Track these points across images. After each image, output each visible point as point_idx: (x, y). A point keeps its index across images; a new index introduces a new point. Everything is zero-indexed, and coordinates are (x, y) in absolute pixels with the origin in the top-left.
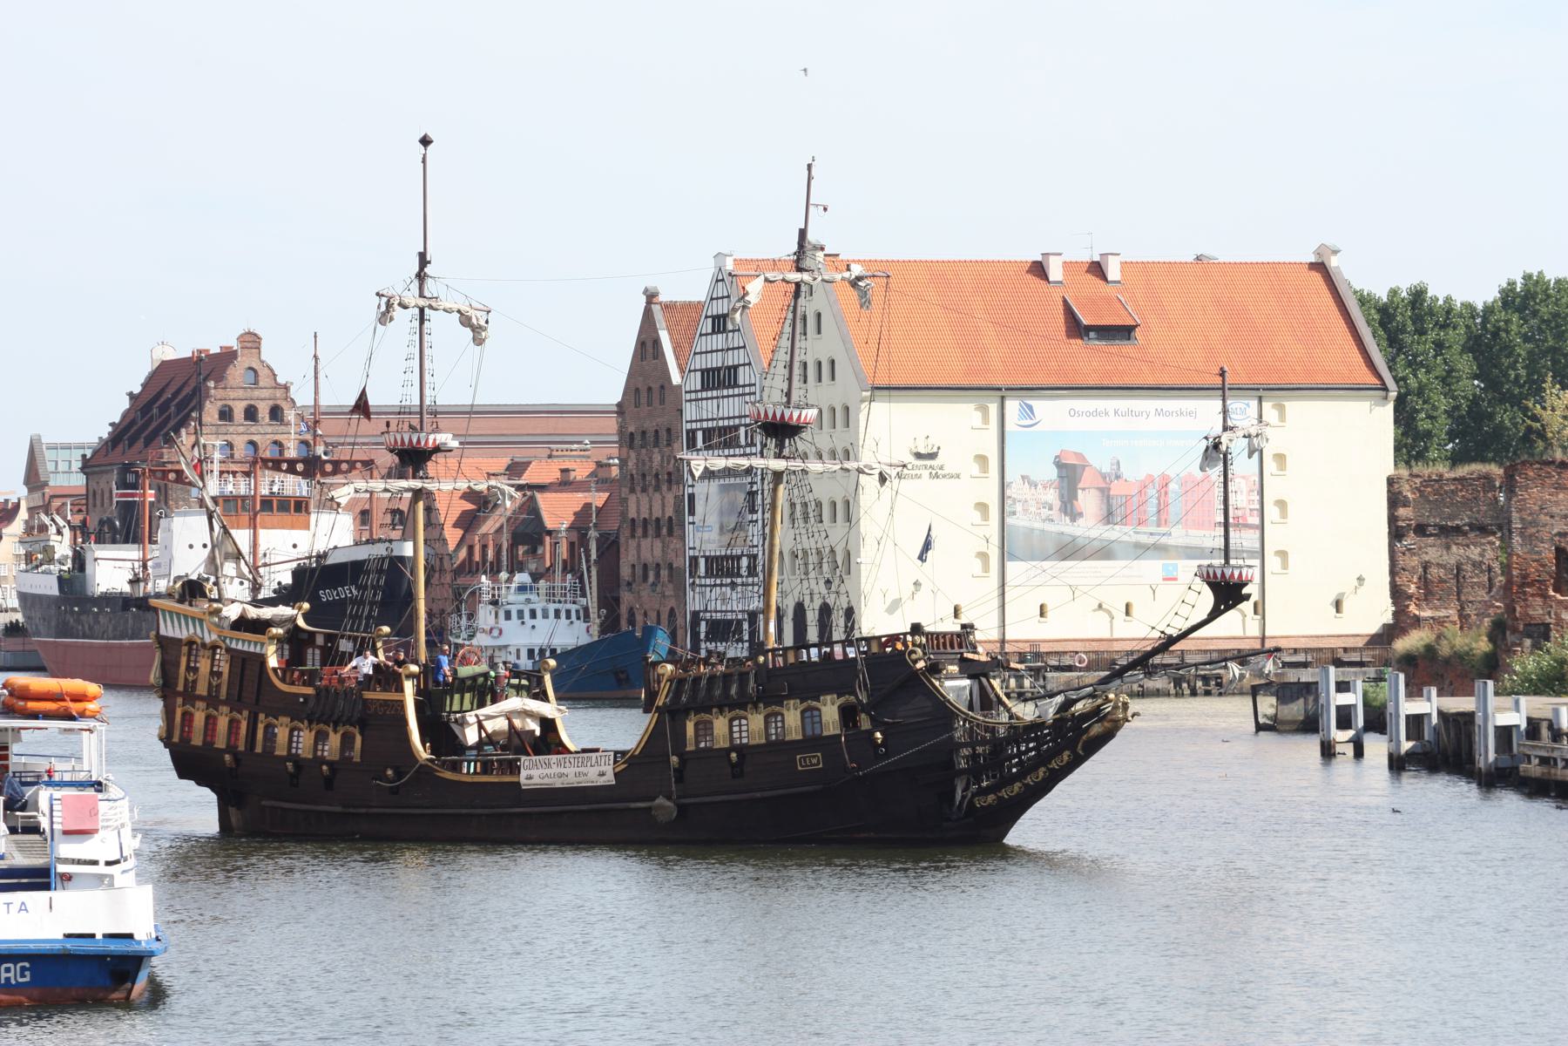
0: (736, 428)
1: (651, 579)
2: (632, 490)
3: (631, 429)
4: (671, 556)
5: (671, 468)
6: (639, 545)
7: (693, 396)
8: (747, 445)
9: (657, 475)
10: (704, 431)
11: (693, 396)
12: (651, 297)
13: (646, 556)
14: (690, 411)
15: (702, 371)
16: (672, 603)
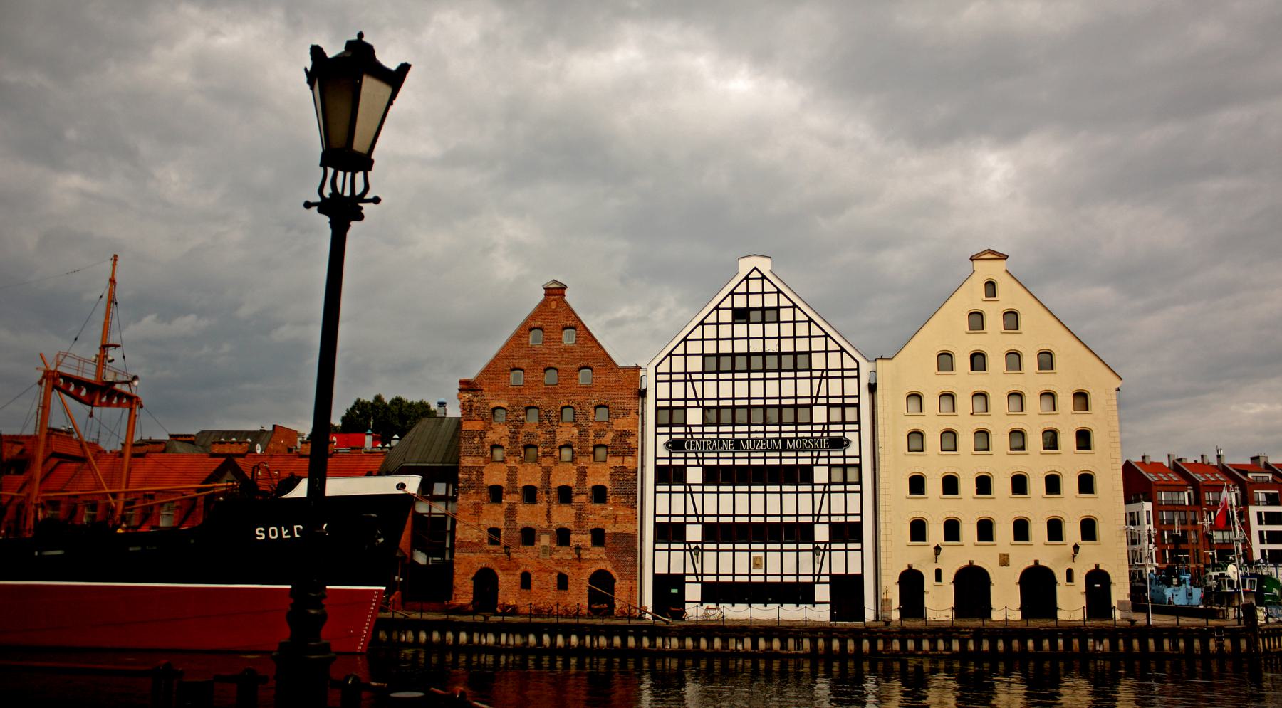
0: (810, 406)
1: (545, 540)
2: (491, 460)
3: (504, 404)
4: (593, 522)
5: (607, 439)
6: (511, 513)
7: (682, 377)
8: (829, 423)
9: (561, 448)
10: (706, 409)
11: (682, 377)
12: (555, 292)
13: (538, 522)
14: (659, 393)
15: (704, 356)
16: (606, 566)
